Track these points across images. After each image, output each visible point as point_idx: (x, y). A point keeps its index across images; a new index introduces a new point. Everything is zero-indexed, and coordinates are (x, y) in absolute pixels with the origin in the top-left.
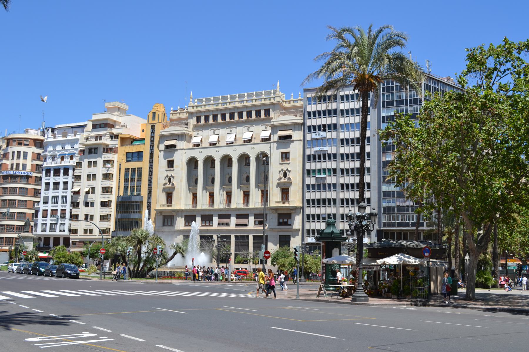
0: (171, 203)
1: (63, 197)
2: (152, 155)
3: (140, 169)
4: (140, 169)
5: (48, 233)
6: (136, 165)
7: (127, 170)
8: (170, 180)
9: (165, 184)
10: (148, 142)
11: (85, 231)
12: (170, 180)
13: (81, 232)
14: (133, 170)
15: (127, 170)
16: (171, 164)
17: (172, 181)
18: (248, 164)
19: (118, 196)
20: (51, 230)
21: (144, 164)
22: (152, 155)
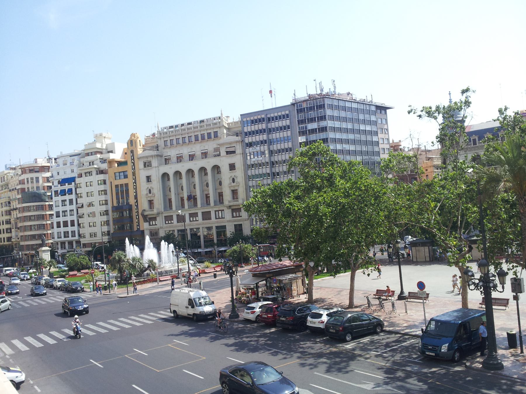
0: (237, 198)
1: (70, 211)
2: (134, 174)
3: (127, 185)
4: (127, 185)
5: (63, 239)
6: (123, 181)
7: (117, 186)
8: (150, 191)
9: (147, 194)
10: (130, 164)
11: (91, 236)
12: (150, 191)
13: (87, 236)
14: (122, 185)
15: (117, 186)
16: (149, 179)
17: (152, 192)
18: (206, 174)
19: (113, 207)
20: (65, 237)
21: (130, 181)
22: (134, 174)
